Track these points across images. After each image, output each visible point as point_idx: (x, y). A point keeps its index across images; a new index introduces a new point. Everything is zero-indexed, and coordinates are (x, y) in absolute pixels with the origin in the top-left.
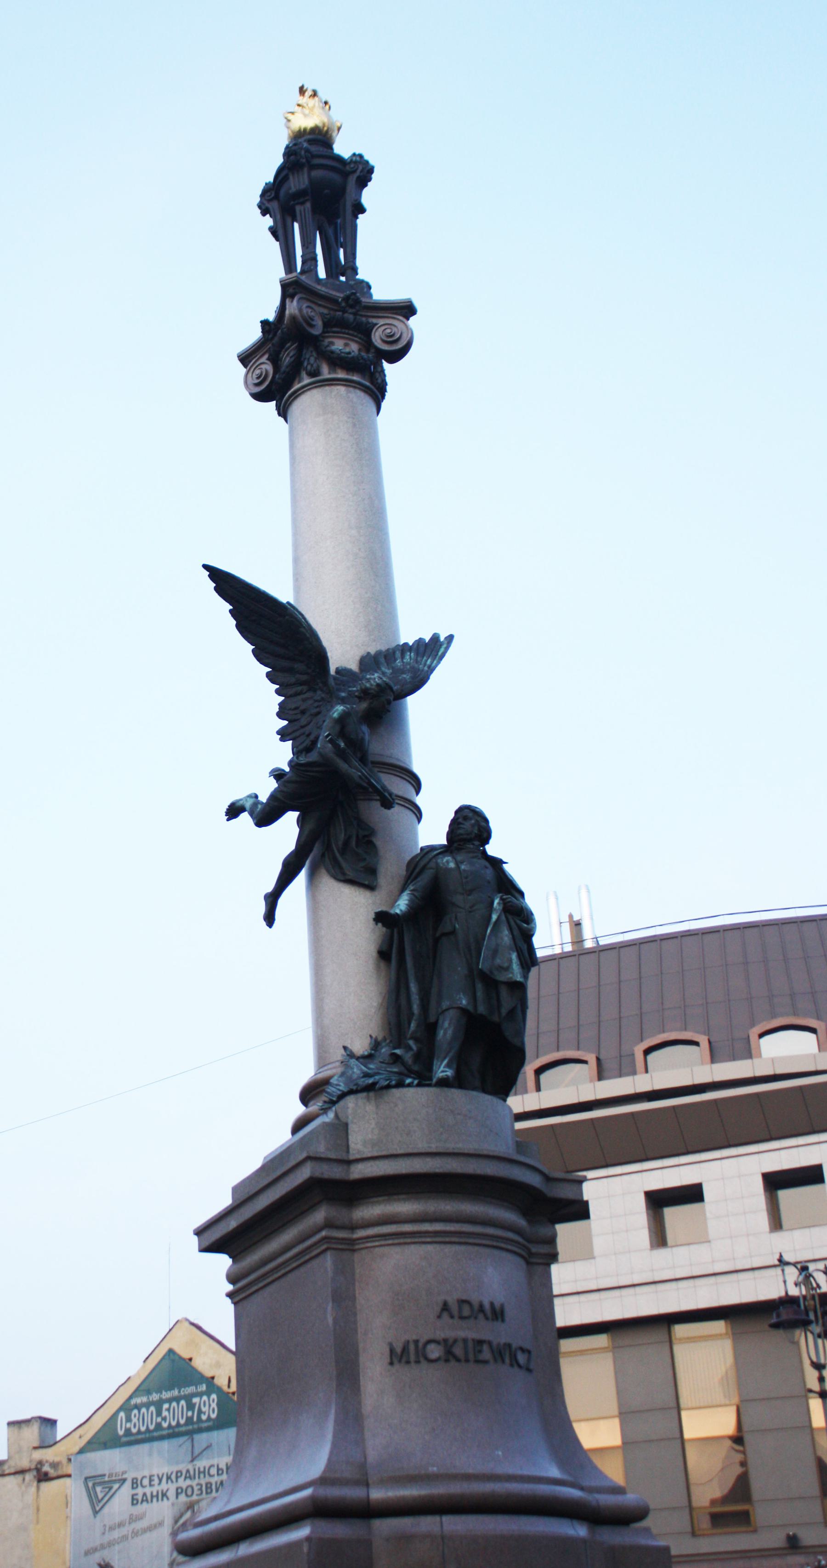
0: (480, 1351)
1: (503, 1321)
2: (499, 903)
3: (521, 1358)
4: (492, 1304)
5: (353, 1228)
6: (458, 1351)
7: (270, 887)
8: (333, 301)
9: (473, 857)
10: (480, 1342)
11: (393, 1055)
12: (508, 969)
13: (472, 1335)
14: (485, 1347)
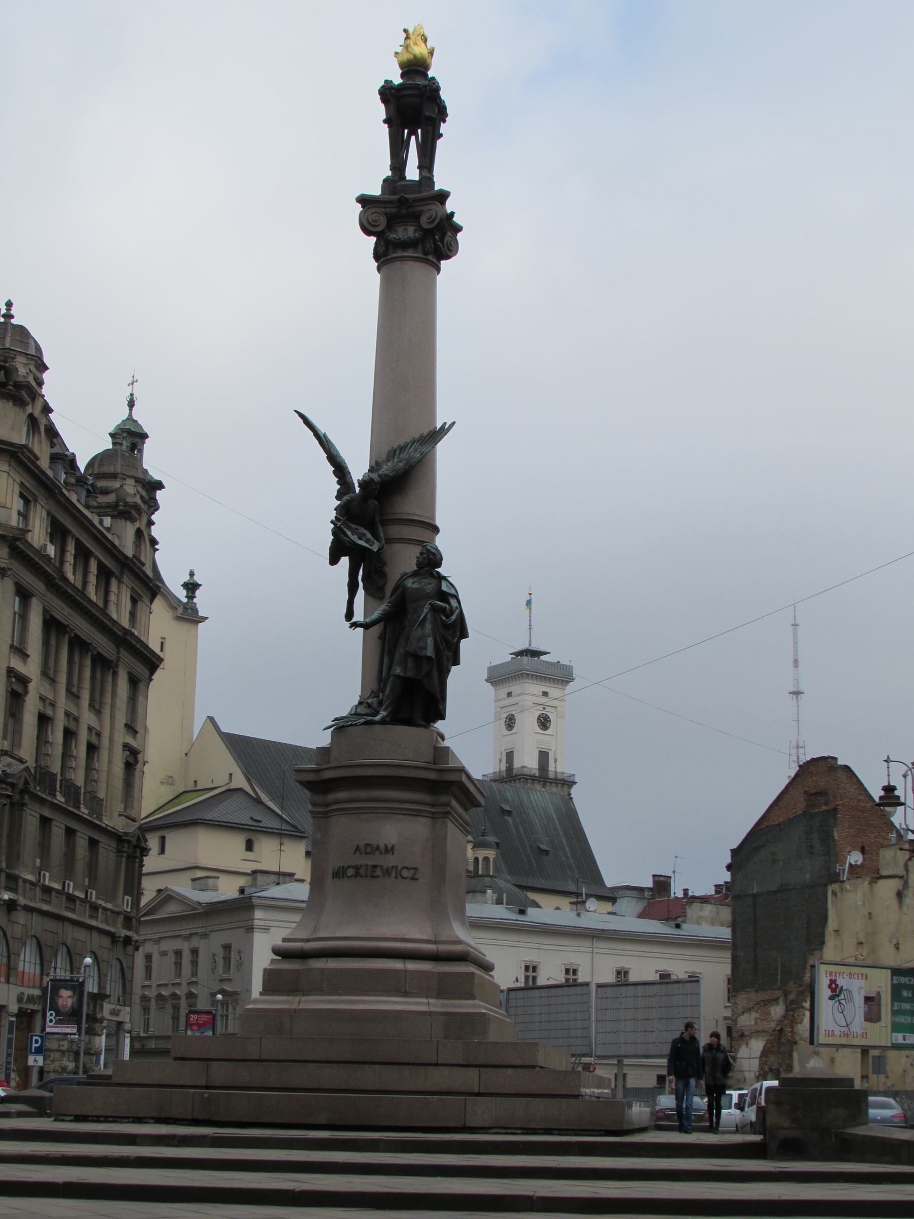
0: (374, 871)
1: (393, 854)
2: (427, 608)
3: (405, 873)
4: (386, 845)
5: (327, 805)
6: (362, 871)
7: (346, 596)
8: (391, 202)
9: (422, 578)
10: (375, 866)
11: (367, 703)
12: (425, 648)
13: (371, 863)
14: (378, 869)
